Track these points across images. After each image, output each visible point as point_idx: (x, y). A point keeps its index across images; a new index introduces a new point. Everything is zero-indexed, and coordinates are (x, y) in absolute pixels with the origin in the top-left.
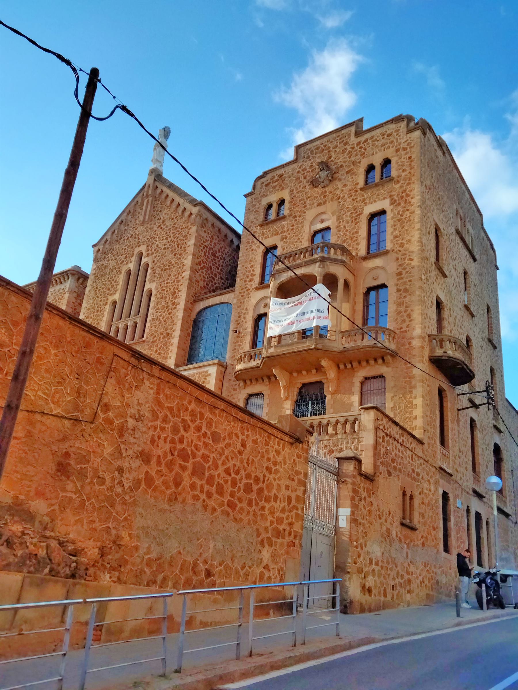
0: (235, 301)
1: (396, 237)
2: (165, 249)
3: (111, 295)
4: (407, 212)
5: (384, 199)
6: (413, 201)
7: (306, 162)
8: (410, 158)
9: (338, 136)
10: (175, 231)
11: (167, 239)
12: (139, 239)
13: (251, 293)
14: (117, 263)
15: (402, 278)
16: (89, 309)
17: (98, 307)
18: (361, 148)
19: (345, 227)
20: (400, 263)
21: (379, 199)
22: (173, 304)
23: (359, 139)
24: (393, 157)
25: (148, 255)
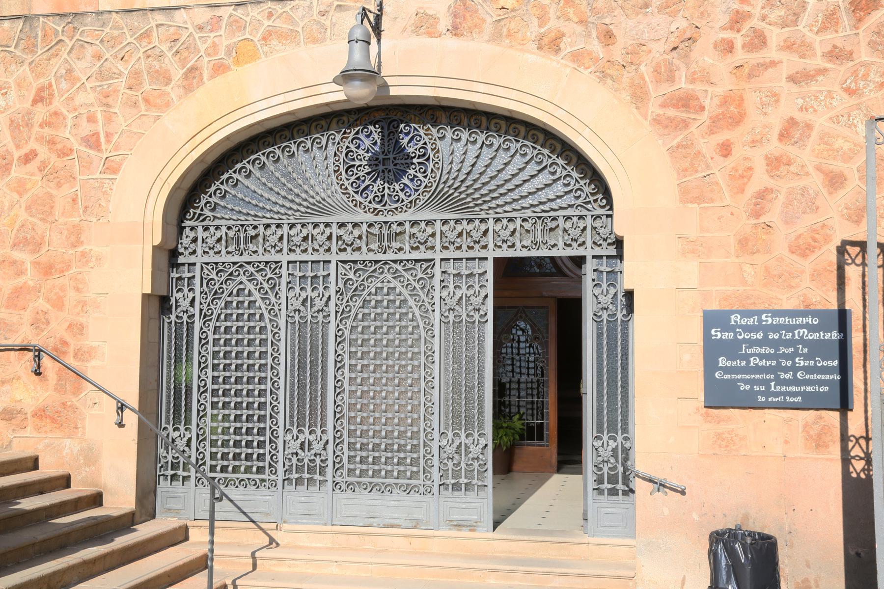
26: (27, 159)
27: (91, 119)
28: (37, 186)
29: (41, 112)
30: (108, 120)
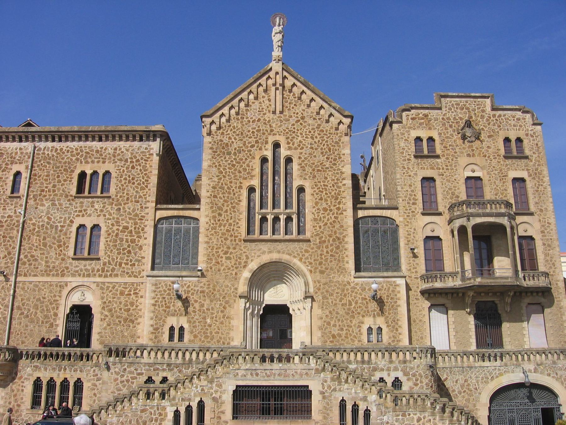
0: (401, 219)
1: (536, 203)
2: (312, 148)
3: (245, 179)
4: (540, 187)
5: (523, 170)
6: (545, 179)
7: (449, 112)
8: (537, 144)
9: (475, 102)
10: (322, 134)
11: (312, 138)
12: (270, 126)
13: (417, 216)
14: (244, 145)
15: (545, 236)
16: (214, 188)
17: (228, 188)
18: (496, 120)
19: (495, 182)
20: (542, 224)
21: (519, 170)
22: (338, 209)
23: (494, 112)
24: (525, 139)
25: (290, 148)
26: (464, 392)
27: (475, 385)
28: (467, 397)
29: (466, 384)
30: (478, 385)
